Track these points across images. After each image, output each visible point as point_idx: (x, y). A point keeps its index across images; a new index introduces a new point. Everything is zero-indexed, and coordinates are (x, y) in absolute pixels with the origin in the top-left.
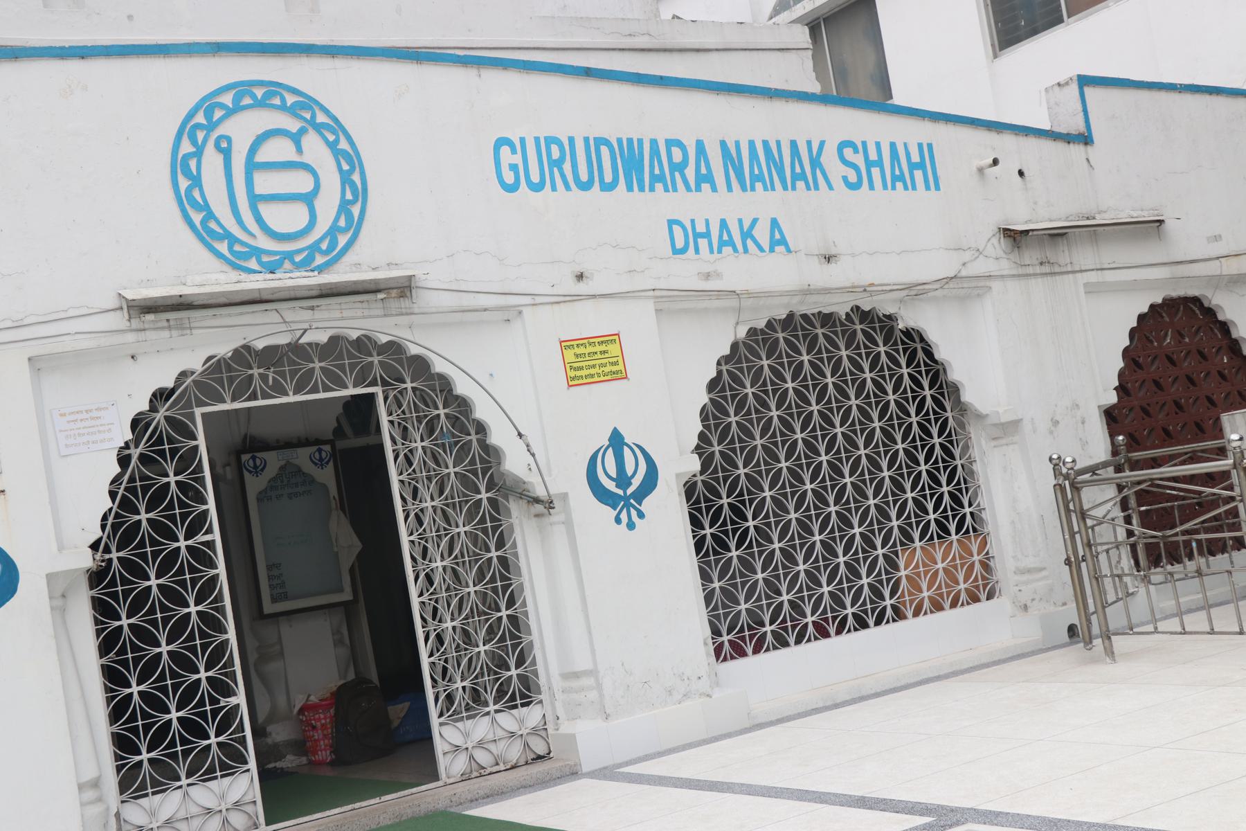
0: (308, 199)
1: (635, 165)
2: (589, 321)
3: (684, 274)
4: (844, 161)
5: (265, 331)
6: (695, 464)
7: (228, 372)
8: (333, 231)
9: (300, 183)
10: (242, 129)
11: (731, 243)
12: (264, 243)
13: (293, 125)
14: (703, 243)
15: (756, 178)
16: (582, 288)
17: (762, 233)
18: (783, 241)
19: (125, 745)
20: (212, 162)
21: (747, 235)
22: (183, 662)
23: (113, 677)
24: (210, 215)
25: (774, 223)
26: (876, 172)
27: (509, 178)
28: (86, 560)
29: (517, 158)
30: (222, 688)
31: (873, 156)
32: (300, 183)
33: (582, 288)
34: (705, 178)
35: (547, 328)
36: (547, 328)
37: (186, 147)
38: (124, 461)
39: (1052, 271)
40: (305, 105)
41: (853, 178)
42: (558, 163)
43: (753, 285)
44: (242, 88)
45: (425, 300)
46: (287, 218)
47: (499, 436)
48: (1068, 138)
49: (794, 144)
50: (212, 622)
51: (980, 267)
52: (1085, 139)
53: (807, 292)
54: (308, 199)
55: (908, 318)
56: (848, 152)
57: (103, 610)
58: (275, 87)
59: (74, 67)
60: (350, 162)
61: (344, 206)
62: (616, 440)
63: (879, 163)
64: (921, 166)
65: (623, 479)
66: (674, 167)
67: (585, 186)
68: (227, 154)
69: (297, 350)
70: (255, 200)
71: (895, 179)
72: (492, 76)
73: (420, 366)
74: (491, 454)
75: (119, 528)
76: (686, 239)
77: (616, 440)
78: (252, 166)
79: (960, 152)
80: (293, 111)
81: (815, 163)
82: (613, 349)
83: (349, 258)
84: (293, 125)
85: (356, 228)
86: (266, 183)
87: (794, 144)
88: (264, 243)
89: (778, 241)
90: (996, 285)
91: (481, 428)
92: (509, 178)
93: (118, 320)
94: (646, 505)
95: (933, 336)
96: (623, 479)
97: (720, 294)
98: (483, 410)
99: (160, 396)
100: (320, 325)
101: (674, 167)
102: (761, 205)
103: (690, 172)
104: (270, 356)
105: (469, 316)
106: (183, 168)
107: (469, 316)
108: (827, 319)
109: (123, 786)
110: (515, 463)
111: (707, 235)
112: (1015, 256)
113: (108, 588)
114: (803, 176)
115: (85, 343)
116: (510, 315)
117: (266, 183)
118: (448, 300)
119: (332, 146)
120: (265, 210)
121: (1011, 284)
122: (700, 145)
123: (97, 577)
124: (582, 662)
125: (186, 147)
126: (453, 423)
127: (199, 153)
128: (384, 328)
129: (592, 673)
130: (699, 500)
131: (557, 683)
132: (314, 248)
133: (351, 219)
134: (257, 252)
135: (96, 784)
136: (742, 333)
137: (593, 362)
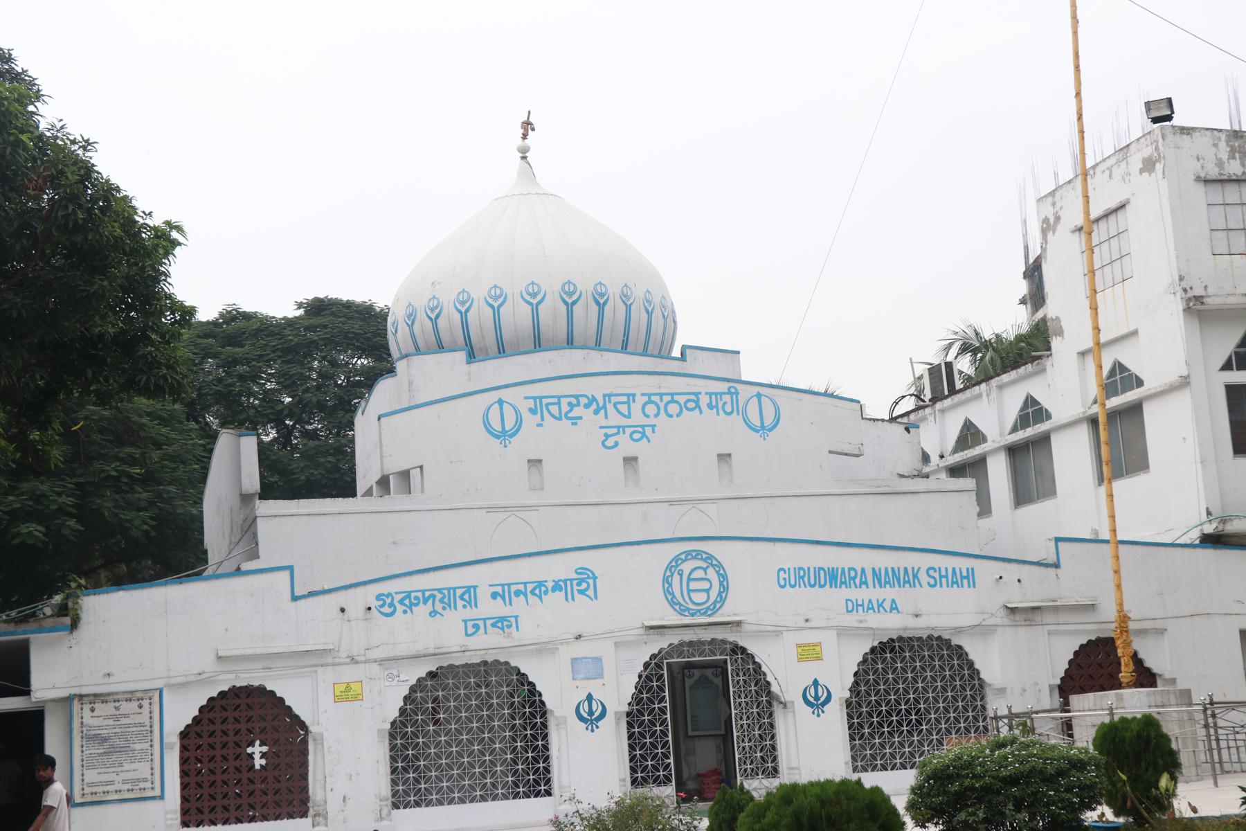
0: (707, 591)
1: (834, 577)
2: (809, 637)
3: (851, 620)
4: (929, 576)
5: (689, 636)
6: (848, 695)
8: (715, 602)
9: (705, 585)
10: (687, 567)
11: (873, 608)
12: (691, 606)
13: (704, 565)
14: (860, 609)
15: (886, 583)
16: (808, 625)
17: (887, 605)
18: (896, 608)
19: (633, 770)
20: (676, 578)
21: (880, 605)
22: (654, 746)
23: (631, 748)
24: (674, 597)
25: (893, 601)
26: (944, 580)
27: (782, 583)
28: (626, 708)
29: (786, 576)
30: (666, 756)
31: (943, 573)
32: (705, 585)
33: (808, 625)
34: (864, 583)
35: (791, 640)
36: (791, 640)
37: (668, 574)
38: (640, 677)
39: (1030, 623)
40: (711, 557)
41: (932, 582)
42: (802, 578)
43: (881, 626)
44: (688, 553)
45: (745, 627)
46: (699, 598)
47: (770, 678)
48: (1047, 566)
49: (906, 569)
50: (664, 734)
51: (992, 621)
53: (905, 629)
54: (707, 591)
55: (955, 642)
56: (931, 572)
57: (630, 725)
58: (699, 552)
59: (636, 548)
60: (723, 577)
61: (720, 594)
62: (816, 683)
63: (946, 576)
64: (967, 577)
65: (817, 698)
66: (851, 578)
67: (812, 586)
68: (681, 575)
69: (701, 643)
70: (689, 591)
71: (953, 583)
72: (779, 545)
73: (743, 650)
74: (768, 683)
75: (637, 699)
76: (853, 606)
77: (816, 683)
78: (689, 580)
80: (705, 560)
81: (915, 576)
82: (818, 648)
83: (720, 612)
84: (704, 565)
85: (723, 601)
86: (693, 585)
87: (906, 569)
88: (691, 606)
89: (894, 608)
90: (999, 629)
91: (765, 674)
92: (782, 583)
93: (641, 631)
94: (826, 708)
95: (967, 648)
96: (817, 698)
97: (866, 629)
98: (764, 669)
99: (653, 656)
100: (707, 635)
101: (851, 578)
102: (889, 593)
103: (857, 581)
104: (691, 644)
105: (762, 634)
106: (667, 580)
107: (762, 634)
108: (920, 639)
109: (633, 783)
110: (775, 688)
111: (862, 605)
112: (1012, 617)
113: (632, 718)
114: (909, 582)
115: (632, 638)
116: (778, 634)
117: (693, 585)
118: (754, 628)
119: (717, 572)
120: (692, 595)
121: (1007, 629)
122: (863, 571)
123: (628, 714)
124: (795, 765)
125: (668, 574)
126: (756, 673)
127: (672, 576)
128: (731, 637)
129: (798, 768)
130: (851, 707)
131: (786, 771)
132: (708, 608)
133: (722, 598)
134: (689, 609)
135: (624, 780)
136: (876, 644)
137: (810, 653)
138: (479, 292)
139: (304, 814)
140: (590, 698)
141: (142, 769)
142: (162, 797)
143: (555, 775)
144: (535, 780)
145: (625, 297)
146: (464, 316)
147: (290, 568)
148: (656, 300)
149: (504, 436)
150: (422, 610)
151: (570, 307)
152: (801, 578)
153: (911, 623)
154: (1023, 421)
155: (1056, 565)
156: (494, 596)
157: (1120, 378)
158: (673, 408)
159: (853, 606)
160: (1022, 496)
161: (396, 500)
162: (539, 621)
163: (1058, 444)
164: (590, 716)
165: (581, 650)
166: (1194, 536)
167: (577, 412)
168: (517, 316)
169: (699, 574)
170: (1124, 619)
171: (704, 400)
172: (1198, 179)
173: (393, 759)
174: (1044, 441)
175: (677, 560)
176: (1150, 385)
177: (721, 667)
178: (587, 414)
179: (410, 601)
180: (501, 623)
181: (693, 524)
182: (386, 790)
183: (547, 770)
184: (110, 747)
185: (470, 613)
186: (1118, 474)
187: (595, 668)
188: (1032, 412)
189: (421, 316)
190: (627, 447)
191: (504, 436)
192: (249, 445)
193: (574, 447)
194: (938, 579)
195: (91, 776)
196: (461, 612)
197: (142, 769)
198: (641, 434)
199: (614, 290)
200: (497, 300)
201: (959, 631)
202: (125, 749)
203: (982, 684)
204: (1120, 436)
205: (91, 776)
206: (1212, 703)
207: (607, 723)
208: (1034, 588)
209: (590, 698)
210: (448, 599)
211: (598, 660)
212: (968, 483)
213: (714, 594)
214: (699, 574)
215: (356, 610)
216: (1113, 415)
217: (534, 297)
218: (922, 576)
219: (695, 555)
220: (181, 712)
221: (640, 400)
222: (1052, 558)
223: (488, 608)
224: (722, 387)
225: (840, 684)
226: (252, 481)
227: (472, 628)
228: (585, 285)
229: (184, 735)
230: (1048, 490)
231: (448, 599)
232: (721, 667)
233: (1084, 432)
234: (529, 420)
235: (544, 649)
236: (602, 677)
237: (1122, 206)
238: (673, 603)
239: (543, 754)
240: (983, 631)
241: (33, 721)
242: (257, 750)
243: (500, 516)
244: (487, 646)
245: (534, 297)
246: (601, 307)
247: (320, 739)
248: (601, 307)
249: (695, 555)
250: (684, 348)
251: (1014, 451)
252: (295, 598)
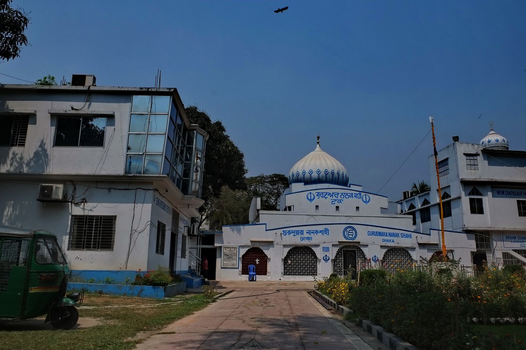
1: (380, 234)
3: (384, 244)
5: (348, 244)
7: (344, 247)
10: (348, 230)
52: (430, 235)
55: (407, 249)
60: (356, 232)
75: (336, 257)
76: (384, 240)
79: (414, 235)
89: (393, 241)
100: (352, 245)
102: (392, 238)
106: (344, 232)
113: (334, 261)
138: (307, 171)
139: (266, 275)
140: (326, 256)
141: (235, 262)
142: (238, 268)
143: (318, 271)
144: (313, 272)
145: (338, 173)
146: (304, 175)
147: (266, 224)
148: (345, 174)
149: (311, 200)
150: (292, 234)
151: (326, 175)
152: (373, 233)
153: (397, 245)
154: (424, 204)
155: (430, 235)
156: (307, 233)
157: (446, 195)
158: (347, 197)
159: (384, 240)
160: (423, 221)
161: (288, 212)
162: (316, 239)
163: (432, 210)
164: (326, 260)
165: (325, 245)
166: (461, 230)
167: (326, 196)
168: (315, 175)
169: (351, 231)
170: (444, 246)
171: (354, 195)
172: (464, 154)
173: (284, 265)
174: (428, 208)
175: (346, 228)
176: (453, 197)
177: (354, 252)
178: (329, 197)
179: (290, 233)
180: (308, 238)
181: (350, 221)
182: (283, 271)
183: (316, 270)
184: (229, 257)
185: (302, 236)
186: (445, 217)
187: (326, 249)
188: (426, 202)
189: (295, 175)
190: (337, 204)
191: (311, 200)
192: (259, 199)
193: (326, 204)
194: (403, 236)
195: (225, 262)
196: (301, 236)
197: (235, 262)
198: (340, 201)
199: (336, 172)
200: (311, 172)
201: (407, 248)
202: (231, 258)
203: (412, 259)
204: (446, 209)
205: (225, 262)
206: (464, 267)
207: (330, 261)
208: (424, 239)
209: (326, 256)
210: (298, 232)
211: (328, 248)
212: (412, 216)
213: (354, 236)
214: (351, 231)
215: (279, 234)
216: (443, 203)
217: (319, 172)
218: (400, 235)
219: (350, 227)
220: (243, 251)
221: (340, 194)
222: (429, 233)
223: (306, 235)
224: (358, 193)
225: (381, 258)
226: (259, 207)
227: (302, 239)
228: (330, 171)
229: (243, 256)
230: (429, 219)
231: (298, 232)
232: (354, 252)
233: (437, 208)
234: (316, 197)
235: (317, 246)
236: (329, 251)
237: (447, 159)
238: (345, 237)
239: (316, 267)
240: (413, 249)
241: (214, 250)
242: (257, 260)
243: (309, 217)
244: (306, 242)
245: (319, 172)
246: (333, 175)
247: (269, 259)
248: (333, 175)
249: (350, 227)
250: (350, 185)
251: (421, 210)
252: (266, 230)
